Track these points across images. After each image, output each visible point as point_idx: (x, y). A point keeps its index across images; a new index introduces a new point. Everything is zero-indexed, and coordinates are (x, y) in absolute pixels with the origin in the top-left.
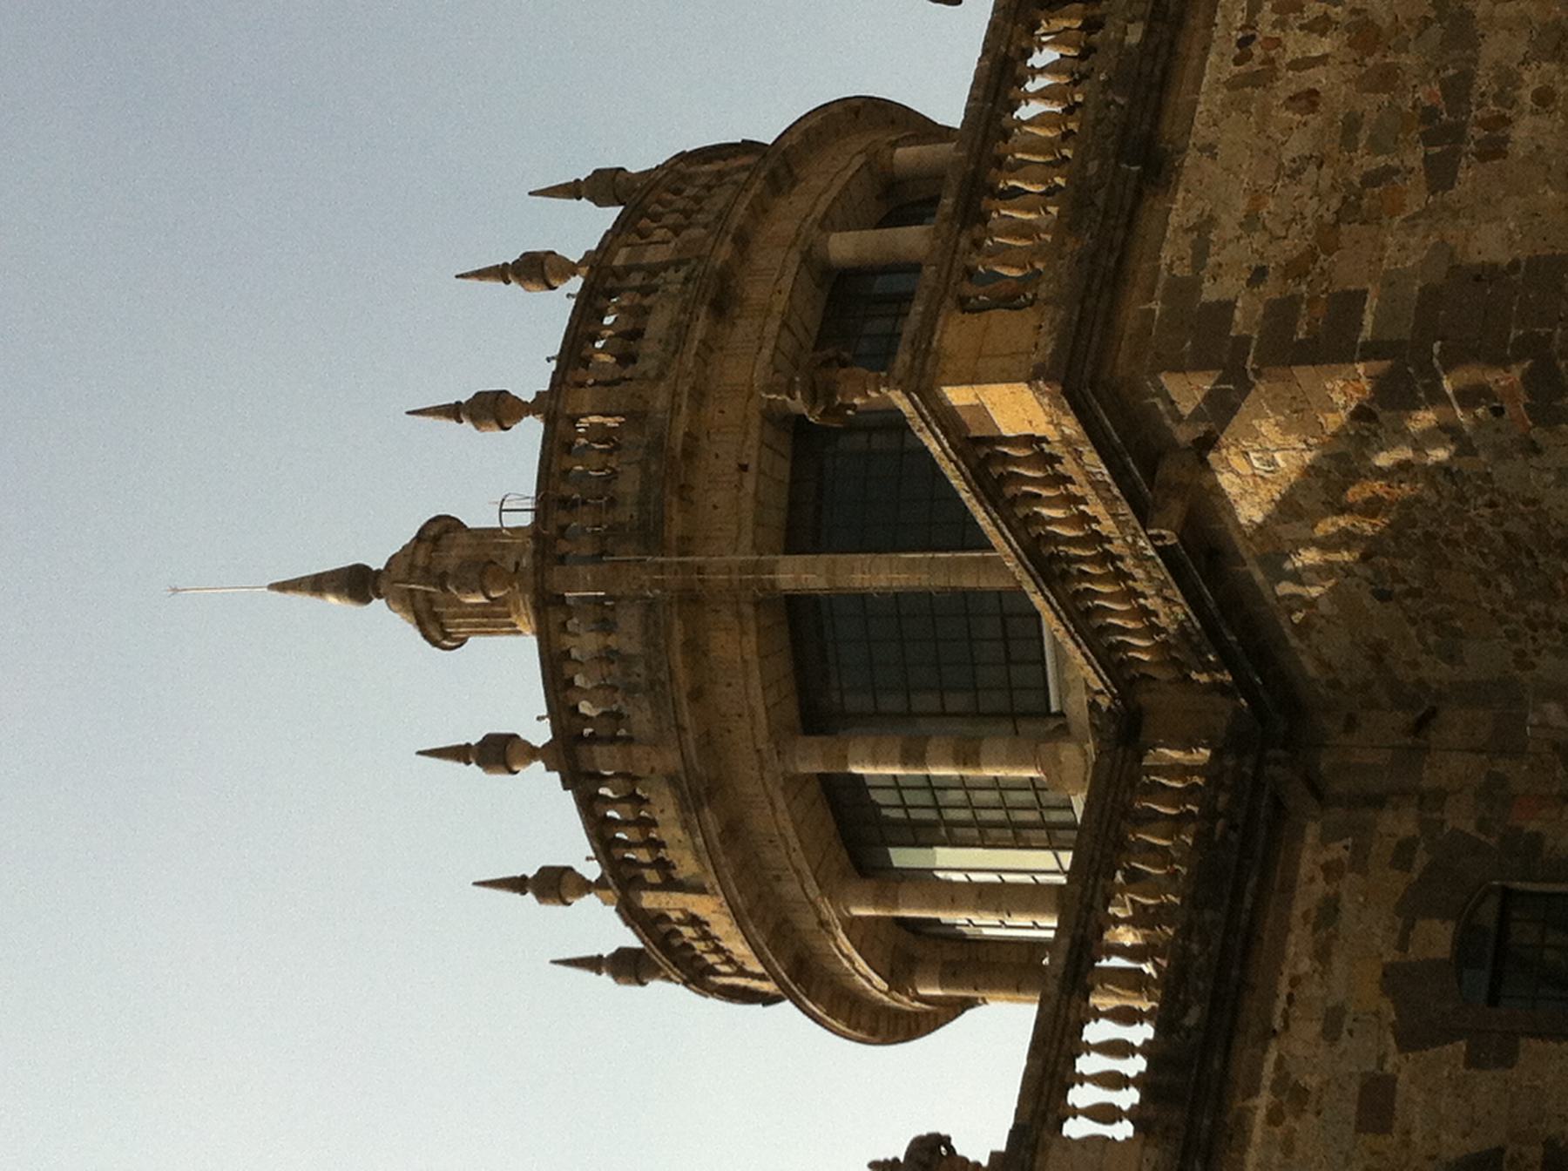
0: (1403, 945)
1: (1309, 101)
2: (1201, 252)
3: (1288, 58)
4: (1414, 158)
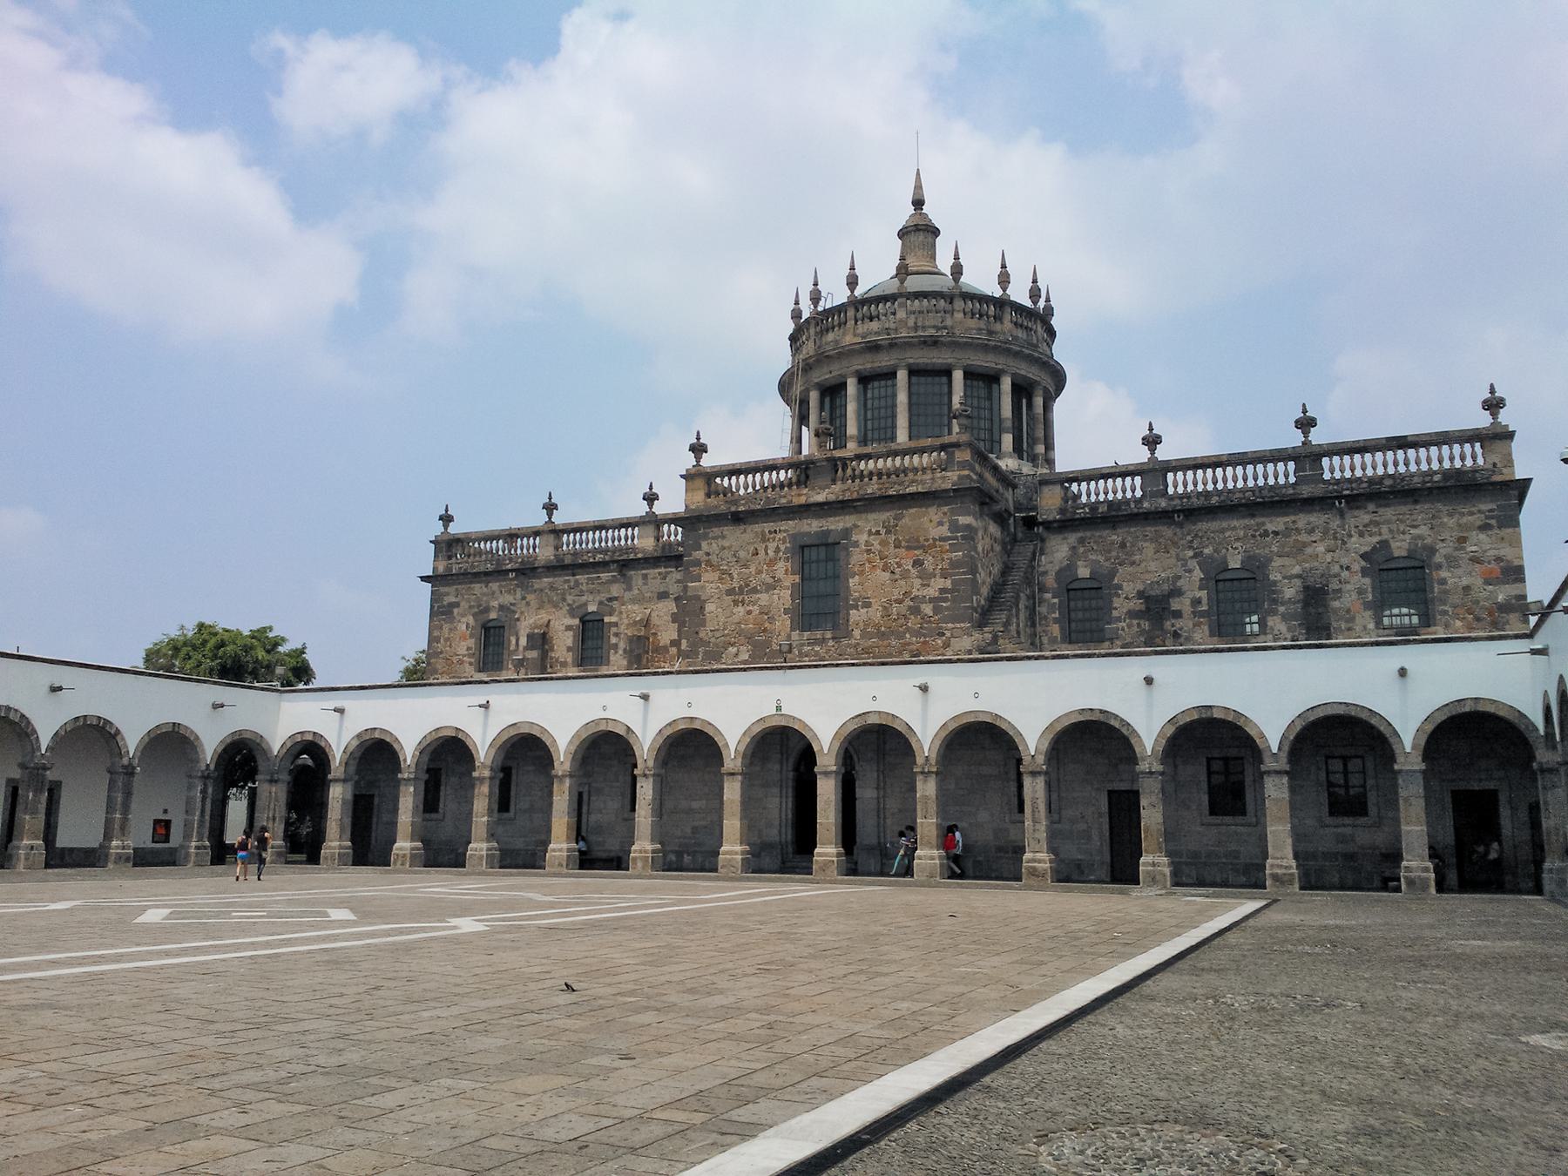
2: (715, 538)
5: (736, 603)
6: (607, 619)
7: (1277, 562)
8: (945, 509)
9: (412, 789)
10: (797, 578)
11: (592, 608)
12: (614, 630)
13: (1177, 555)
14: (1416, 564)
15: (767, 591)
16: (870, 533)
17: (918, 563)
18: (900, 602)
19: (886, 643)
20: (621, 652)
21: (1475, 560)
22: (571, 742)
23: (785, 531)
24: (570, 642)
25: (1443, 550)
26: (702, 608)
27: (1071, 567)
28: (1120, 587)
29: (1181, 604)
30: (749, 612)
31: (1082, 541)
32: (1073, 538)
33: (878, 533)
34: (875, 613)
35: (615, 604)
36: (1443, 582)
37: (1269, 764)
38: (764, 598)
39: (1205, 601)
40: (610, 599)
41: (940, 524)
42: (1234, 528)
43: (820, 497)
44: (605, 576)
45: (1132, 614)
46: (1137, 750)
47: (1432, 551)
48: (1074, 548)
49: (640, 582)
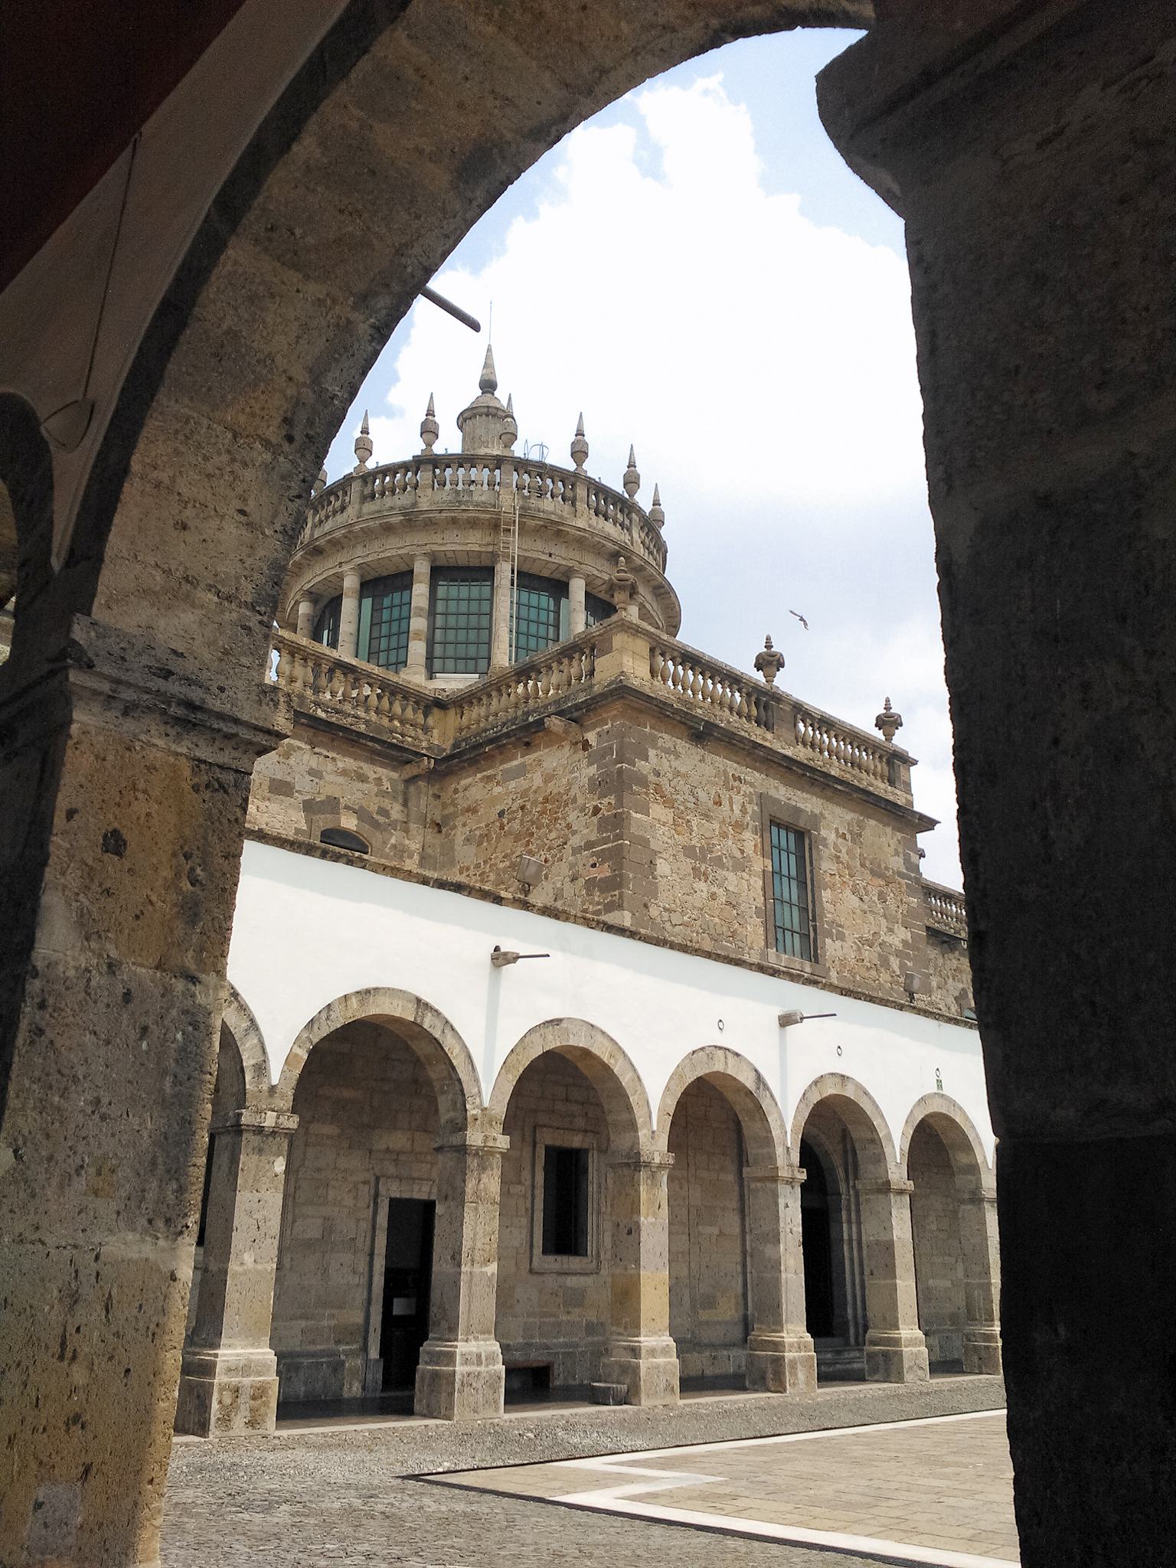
0: (347, 807)
1: (719, 803)
2: (667, 751)
3: (734, 796)
5: (697, 873)
9: (280, 1165)
23: (752, 785)
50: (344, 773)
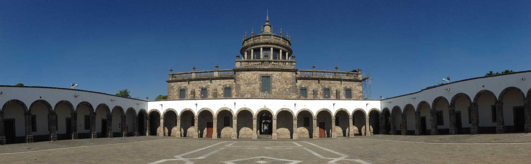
2: (243, 73)
4: (247, 82)
5: (247, 86)
6: (207, 89)
7: (333, 88)
8: (291, 73)
10: (261, 82)
11: (204, 87)
12: (209, 91)
13: (318, 85)
14: (350, 90)
15: (254, 84)
16: (276, 75)
17: (286, 82)
18: (282, 88)
19: (279, 95)
20: (211, 95)
21: (357, 90)
22: (217, 112)
24: (199, 93)
25: (353, 88)
26: (240, 87)
27: (301, 85)
28: (309, 89)
29: (319, 93)
30: (250, 88)
31: (303, 81)
32: (302, 81)
33: (278, 75)
34: (277, 90)
35: (209, 86)
36: (353, 92)
37: (350, 117)
38: (254, 86)
39: (322, 92)
40: (208, 85)
41: (290, 75)
42: (327, 82)
43: (266, 67)
44: (207, 81)
45: (311, 94)
46: (332, 115)
47: (352, 88)
48: (302, 82)
49: (215, 82)
50: (227, 81)
